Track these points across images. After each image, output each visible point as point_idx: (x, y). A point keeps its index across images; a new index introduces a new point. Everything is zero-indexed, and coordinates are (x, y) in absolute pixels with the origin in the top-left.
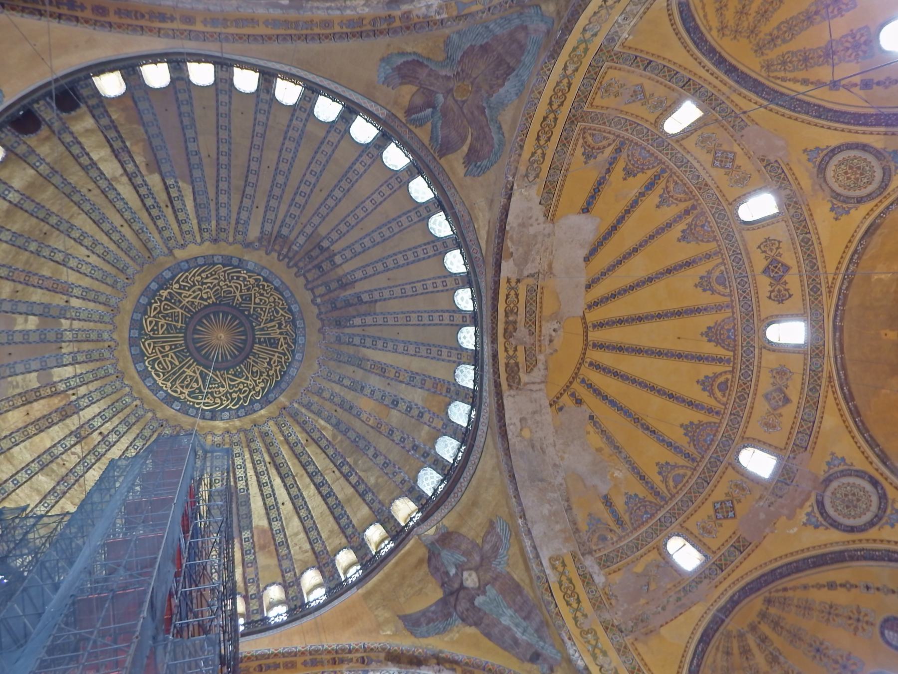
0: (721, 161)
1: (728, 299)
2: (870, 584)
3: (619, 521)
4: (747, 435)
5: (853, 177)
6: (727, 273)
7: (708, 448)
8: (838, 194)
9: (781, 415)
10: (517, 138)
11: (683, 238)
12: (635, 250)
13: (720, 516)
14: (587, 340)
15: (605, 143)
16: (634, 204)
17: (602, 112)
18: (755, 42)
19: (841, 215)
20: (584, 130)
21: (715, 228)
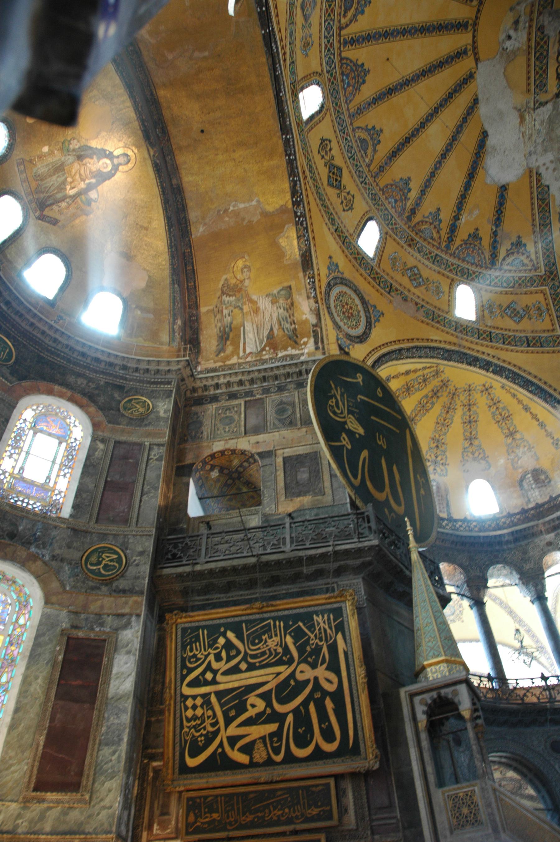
0: (415, 275)
1: (355, 125)
6: (362, 156)
8: (341, 283)
12: (444, 156)
16: (460, 206)
17: (528, 289)
18: (449, 387)
21: (386, 203)
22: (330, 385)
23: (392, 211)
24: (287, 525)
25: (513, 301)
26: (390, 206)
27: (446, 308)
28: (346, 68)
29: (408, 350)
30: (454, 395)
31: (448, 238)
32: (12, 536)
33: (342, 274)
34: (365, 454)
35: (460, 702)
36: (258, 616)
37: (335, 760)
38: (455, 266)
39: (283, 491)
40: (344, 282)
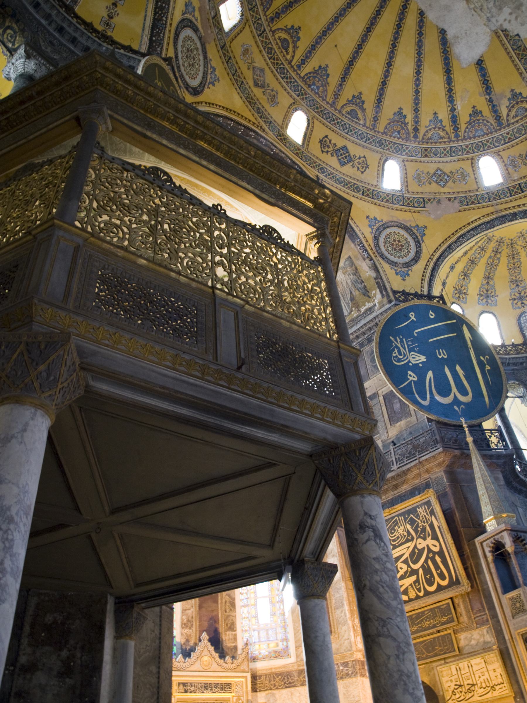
0: (440, 176)
1: (339, 108)
5: (395, 243)
6: (357, 123)
8: (385, 228)
9: (249, 69)
11: (400, 112)
12: (418, 72)
15: (513, 113)
16: (451, 99)
18: (505, 242)
19: (369, 221)
22: (391, 340)
23: (400, 141)
24: (392, 451)
26: (396, 139)
27: (475, 187)
28: (310, 80)
29: (455, 242)
30: (512, 244)
31: (453, 129)
33: (382, 221)
34: (430, 374)
35: (505, 543)
36: (389, 517)
37: (449, 589)
38: (470, 146)
39: (388, 421)
40: (385, 226)
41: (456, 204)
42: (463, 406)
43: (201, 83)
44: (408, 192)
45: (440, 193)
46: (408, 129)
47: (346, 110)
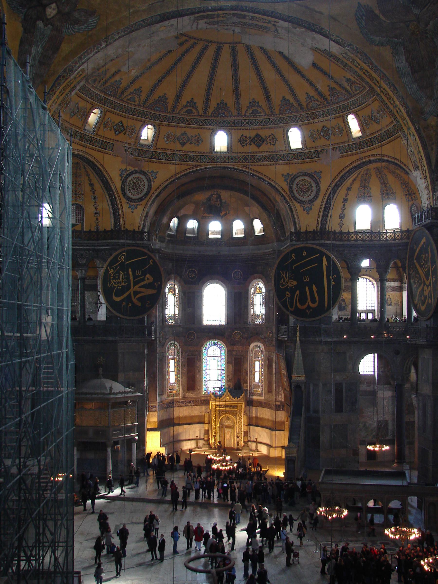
0: (325, 131)
1: (243, 114)
2: (97, 200)
3: (106, 82)
4: (161, 127)
6: (259, 116)
7: (152, 109)
8: (295, 179)
10: (372, 64)
11: (284, 99)
12: (282, 76)
13: (116, 127)
14: (224, 43)
15: (353, 89)
16: (311, 84)
20: (365, 87)
21: (287, 115)
25: (372, 110)
32: (257, 334)
34: (298, 292)
41: (338, 152)
42: (311, 310)
43: (149, 185)
44: (307, 148)
45: (326, 145)
46: (294, 106)
47: (249, 112)
